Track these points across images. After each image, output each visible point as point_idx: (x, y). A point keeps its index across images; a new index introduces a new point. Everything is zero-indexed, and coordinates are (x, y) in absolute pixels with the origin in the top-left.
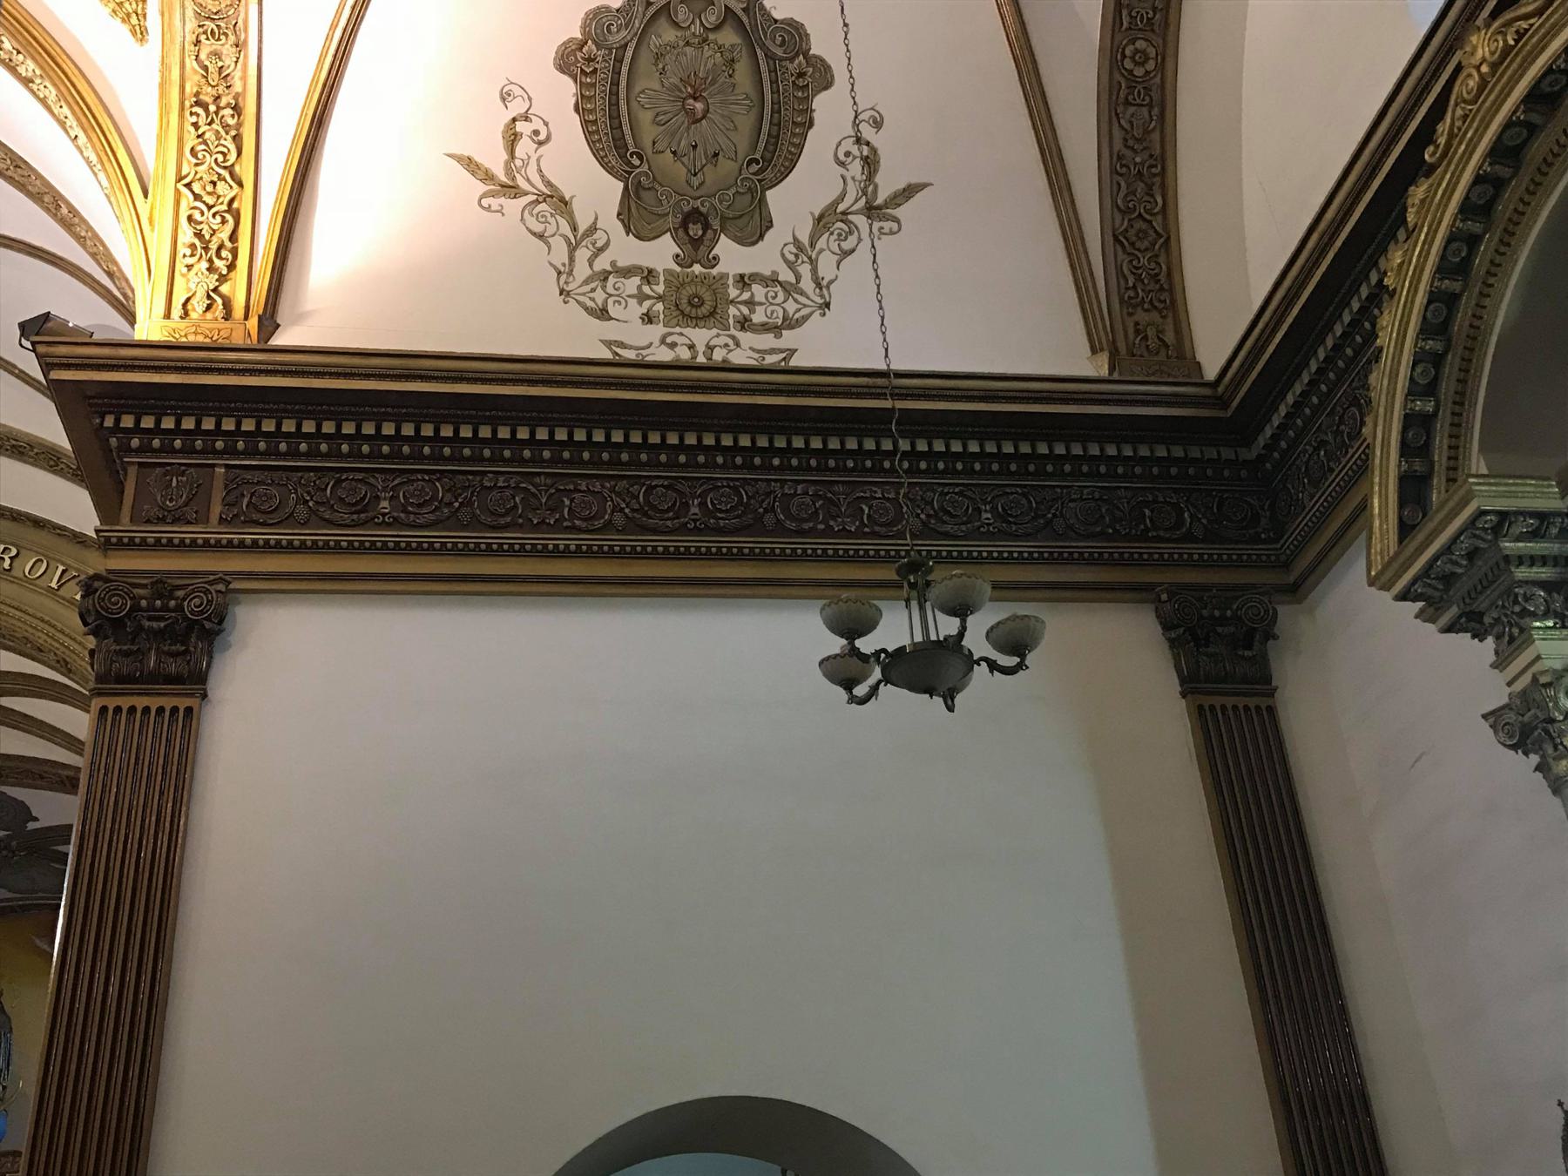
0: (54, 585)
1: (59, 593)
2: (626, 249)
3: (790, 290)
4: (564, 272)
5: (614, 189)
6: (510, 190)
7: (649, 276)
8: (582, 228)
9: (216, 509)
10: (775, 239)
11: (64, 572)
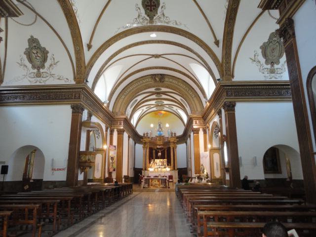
2: (266, 66)
3: (282, 69)
4: (260, 69)
5: (264, 60)
6: (255, 61)
7: (268, 69)
8: (261, 64)
9: (233, 95)
10: (280, 64)
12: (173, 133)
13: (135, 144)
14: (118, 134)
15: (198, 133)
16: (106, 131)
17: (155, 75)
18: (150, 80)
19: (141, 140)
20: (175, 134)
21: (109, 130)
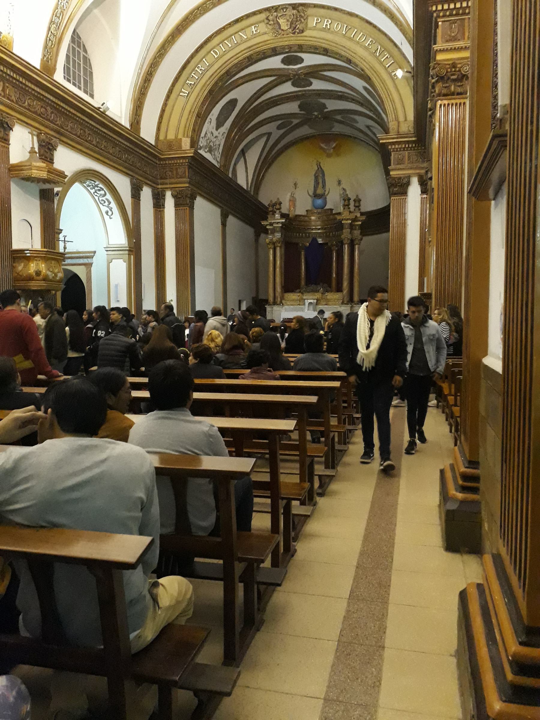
0: (344, 32)
1: (346, 35)
11: (346, 27)
12: (353, 197)
13: (257, 235)
14: (177, 205)
15: (404, 193)
16: (136, 195)
17: (276, 8)
18: (262, 28)
19: (264, 223)
20: (358, 201)
21: (146, 193)
